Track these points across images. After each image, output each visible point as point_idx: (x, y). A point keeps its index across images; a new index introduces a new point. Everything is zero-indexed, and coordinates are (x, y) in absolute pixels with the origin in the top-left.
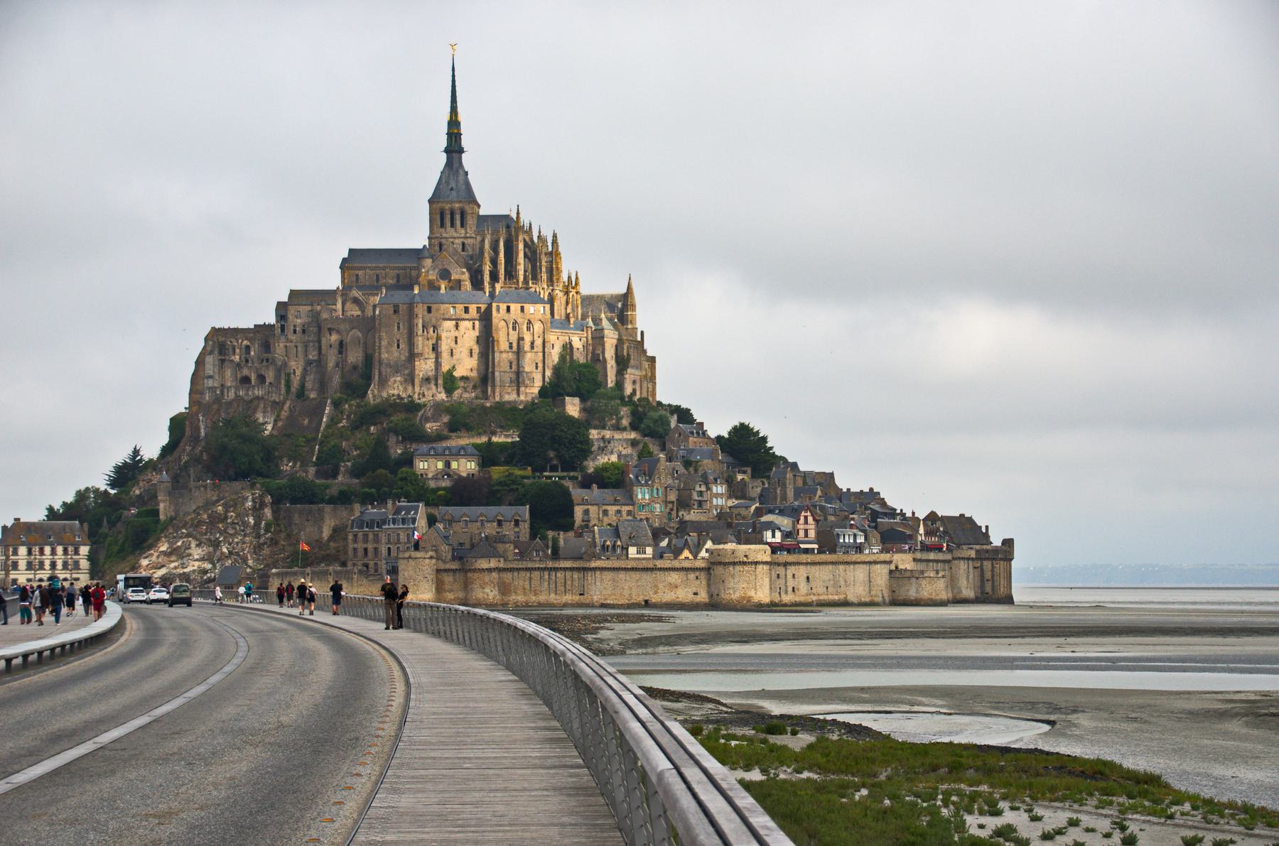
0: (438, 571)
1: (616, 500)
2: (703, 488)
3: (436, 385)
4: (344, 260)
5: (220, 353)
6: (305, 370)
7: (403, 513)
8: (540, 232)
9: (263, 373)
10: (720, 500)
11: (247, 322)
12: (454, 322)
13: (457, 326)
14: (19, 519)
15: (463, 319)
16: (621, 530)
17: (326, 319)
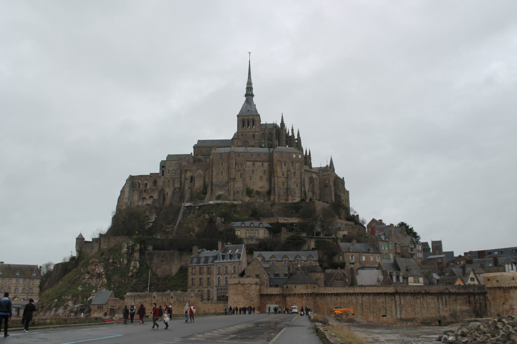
0: (262, 296)
1: (369, 250)
2: (413, 246)
3: (242, 195)
4: (195, 145)
5: (133, 187)
6: (173, 193)
7: (230, 251)
8: (292, 127)
9: (152, 196)
10: (420, 253)
11: (147, 172)
12: (252, 163)
13: (254, 165)
14: (3, 262)
15: (257, 161)
16: (399, 264)
17: (184, 165)
